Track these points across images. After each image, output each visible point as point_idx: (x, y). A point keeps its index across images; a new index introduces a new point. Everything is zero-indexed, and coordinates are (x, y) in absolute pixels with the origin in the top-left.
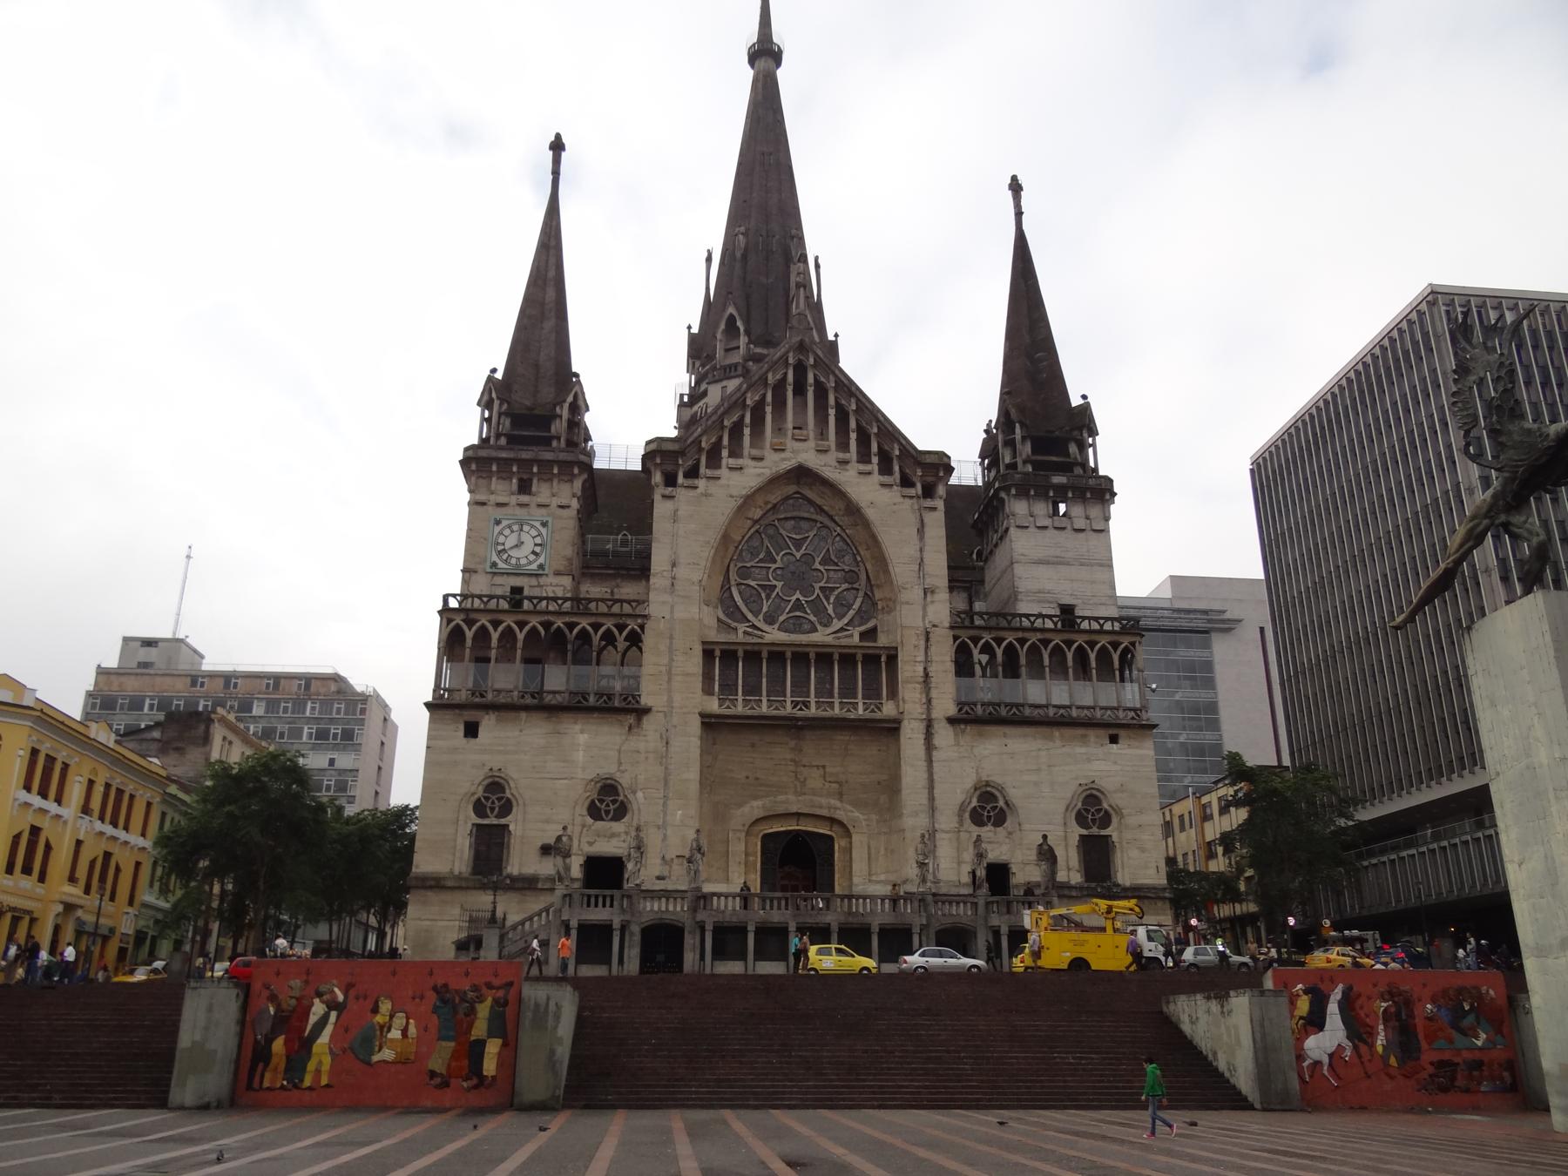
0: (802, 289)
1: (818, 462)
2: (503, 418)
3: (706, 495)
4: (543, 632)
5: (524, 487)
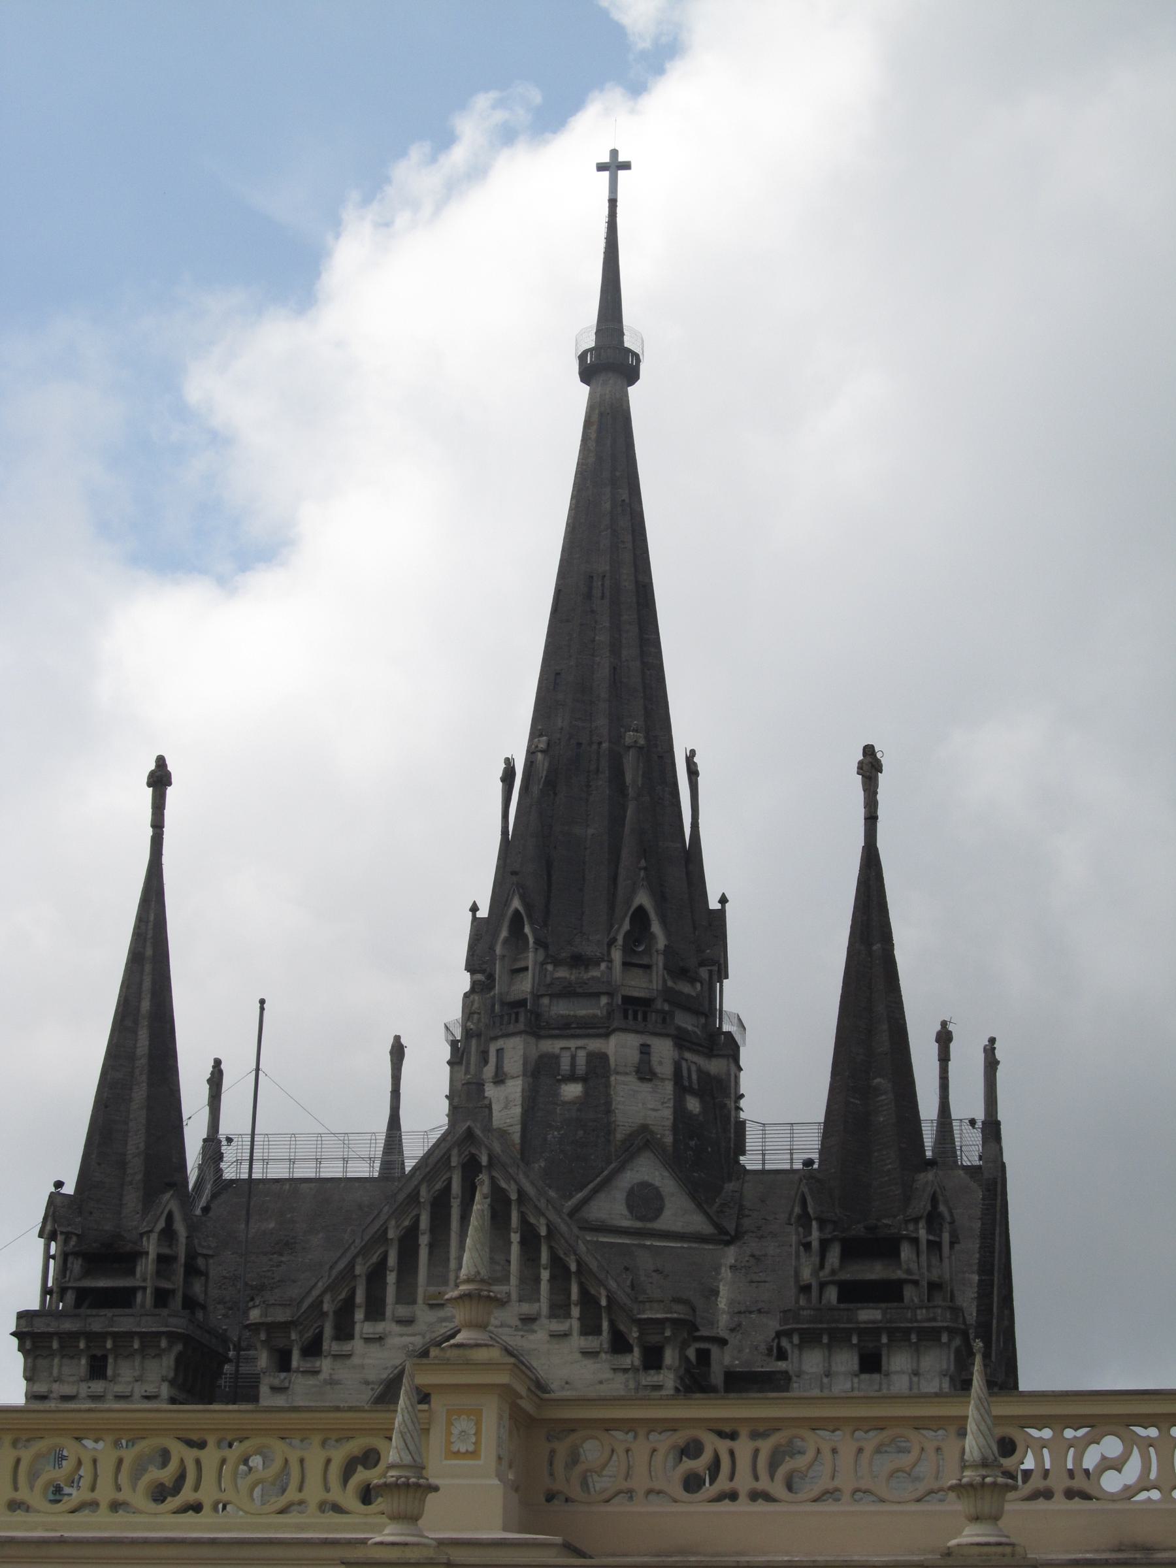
0: (474, 1042)
2: (70, 1259)
3: (332, 1382)
5: (97, 1370)
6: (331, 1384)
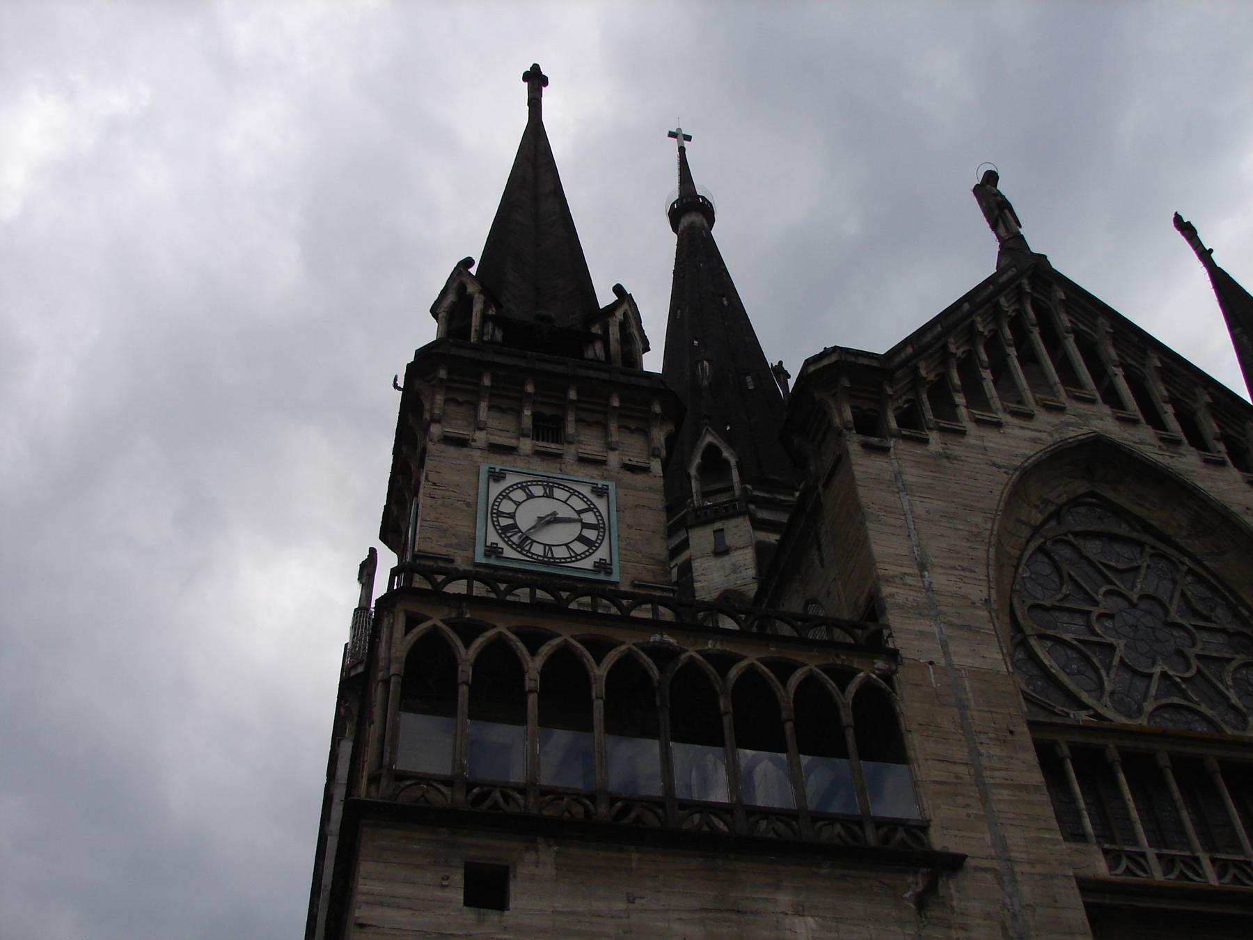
0: (1007, 211)
1: (1126, 435)
4: (655, 672)
6: (947, 457)
